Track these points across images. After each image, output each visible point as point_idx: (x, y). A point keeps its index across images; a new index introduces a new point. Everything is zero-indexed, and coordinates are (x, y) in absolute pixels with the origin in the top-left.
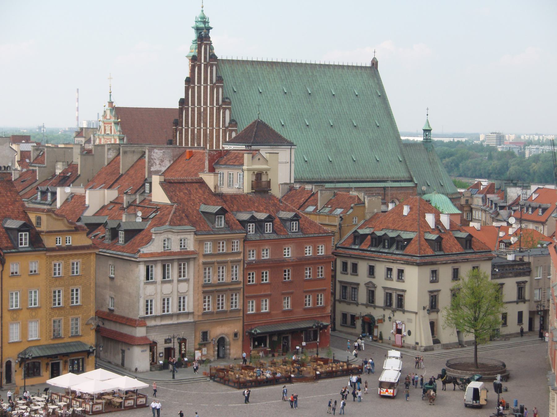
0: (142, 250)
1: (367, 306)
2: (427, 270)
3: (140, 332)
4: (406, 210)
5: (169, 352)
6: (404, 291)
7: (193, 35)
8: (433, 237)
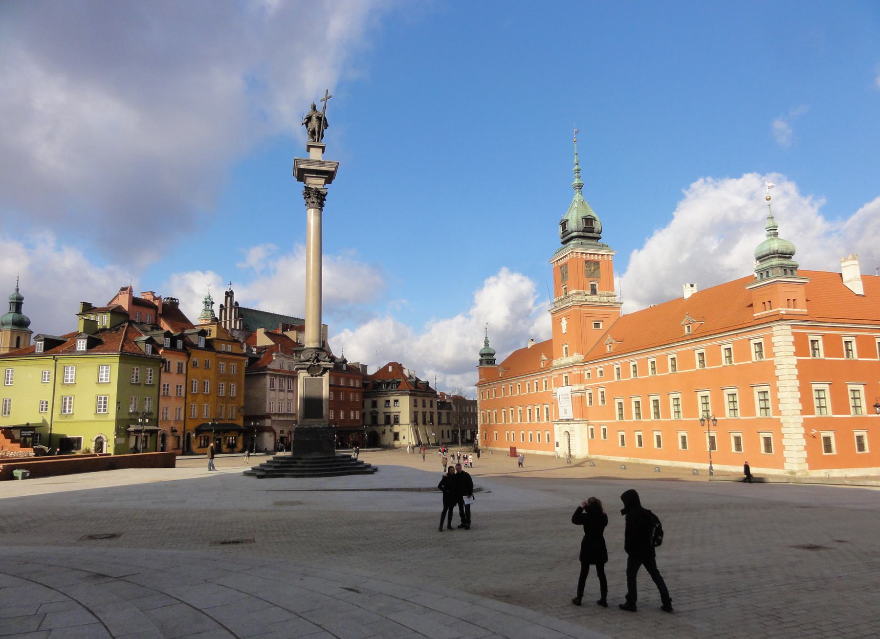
1: (371, 426)
2: (413, 398)
3: (268, 423)
5: (282, 439)
7: (203, 306)
8: (412, 380)
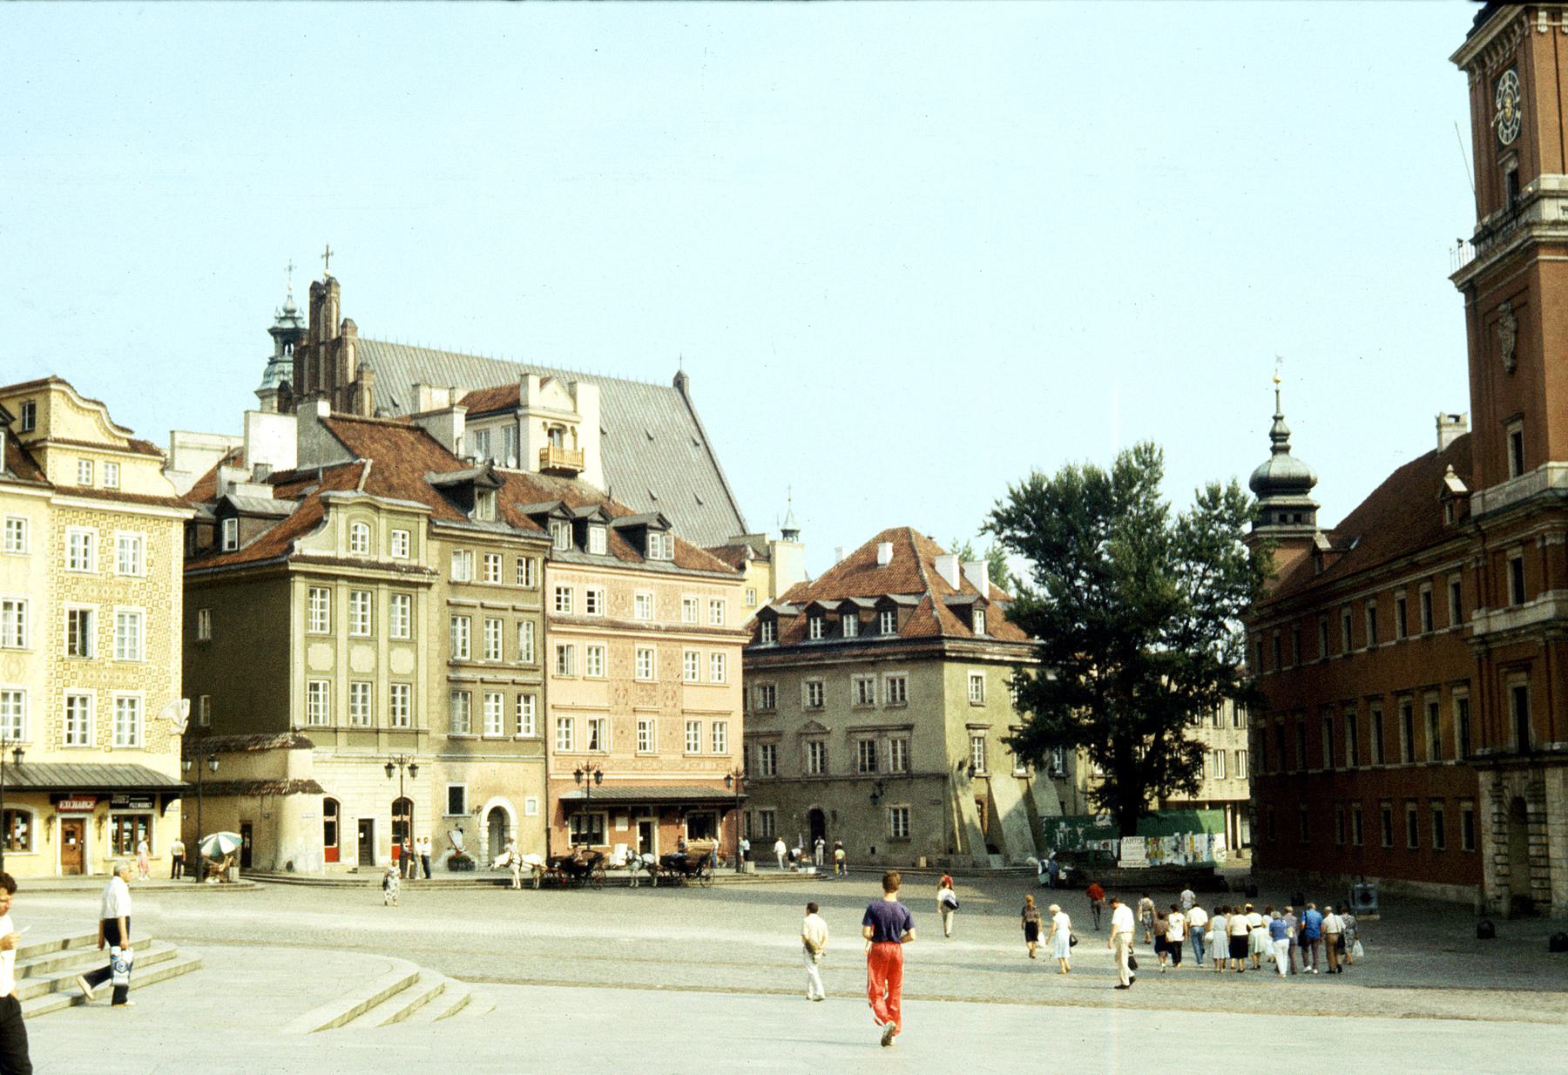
0: (297, 544)
4: (886, 554)
6: (908, 728)
7: (269, 347)
